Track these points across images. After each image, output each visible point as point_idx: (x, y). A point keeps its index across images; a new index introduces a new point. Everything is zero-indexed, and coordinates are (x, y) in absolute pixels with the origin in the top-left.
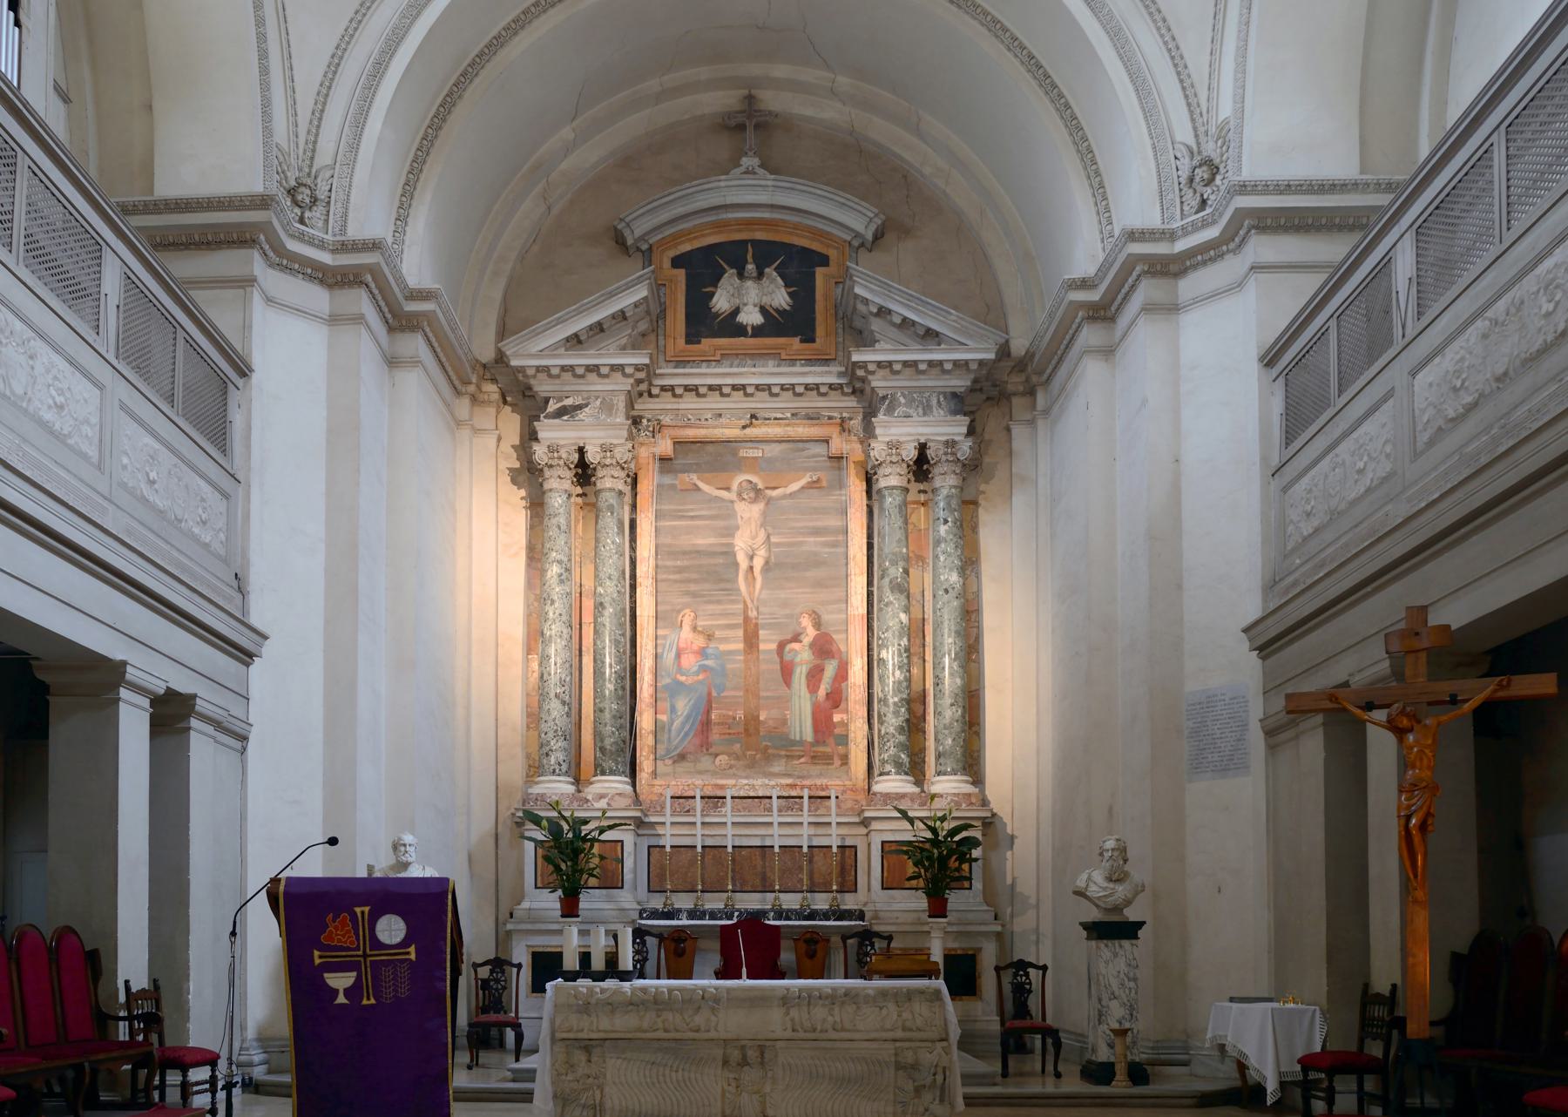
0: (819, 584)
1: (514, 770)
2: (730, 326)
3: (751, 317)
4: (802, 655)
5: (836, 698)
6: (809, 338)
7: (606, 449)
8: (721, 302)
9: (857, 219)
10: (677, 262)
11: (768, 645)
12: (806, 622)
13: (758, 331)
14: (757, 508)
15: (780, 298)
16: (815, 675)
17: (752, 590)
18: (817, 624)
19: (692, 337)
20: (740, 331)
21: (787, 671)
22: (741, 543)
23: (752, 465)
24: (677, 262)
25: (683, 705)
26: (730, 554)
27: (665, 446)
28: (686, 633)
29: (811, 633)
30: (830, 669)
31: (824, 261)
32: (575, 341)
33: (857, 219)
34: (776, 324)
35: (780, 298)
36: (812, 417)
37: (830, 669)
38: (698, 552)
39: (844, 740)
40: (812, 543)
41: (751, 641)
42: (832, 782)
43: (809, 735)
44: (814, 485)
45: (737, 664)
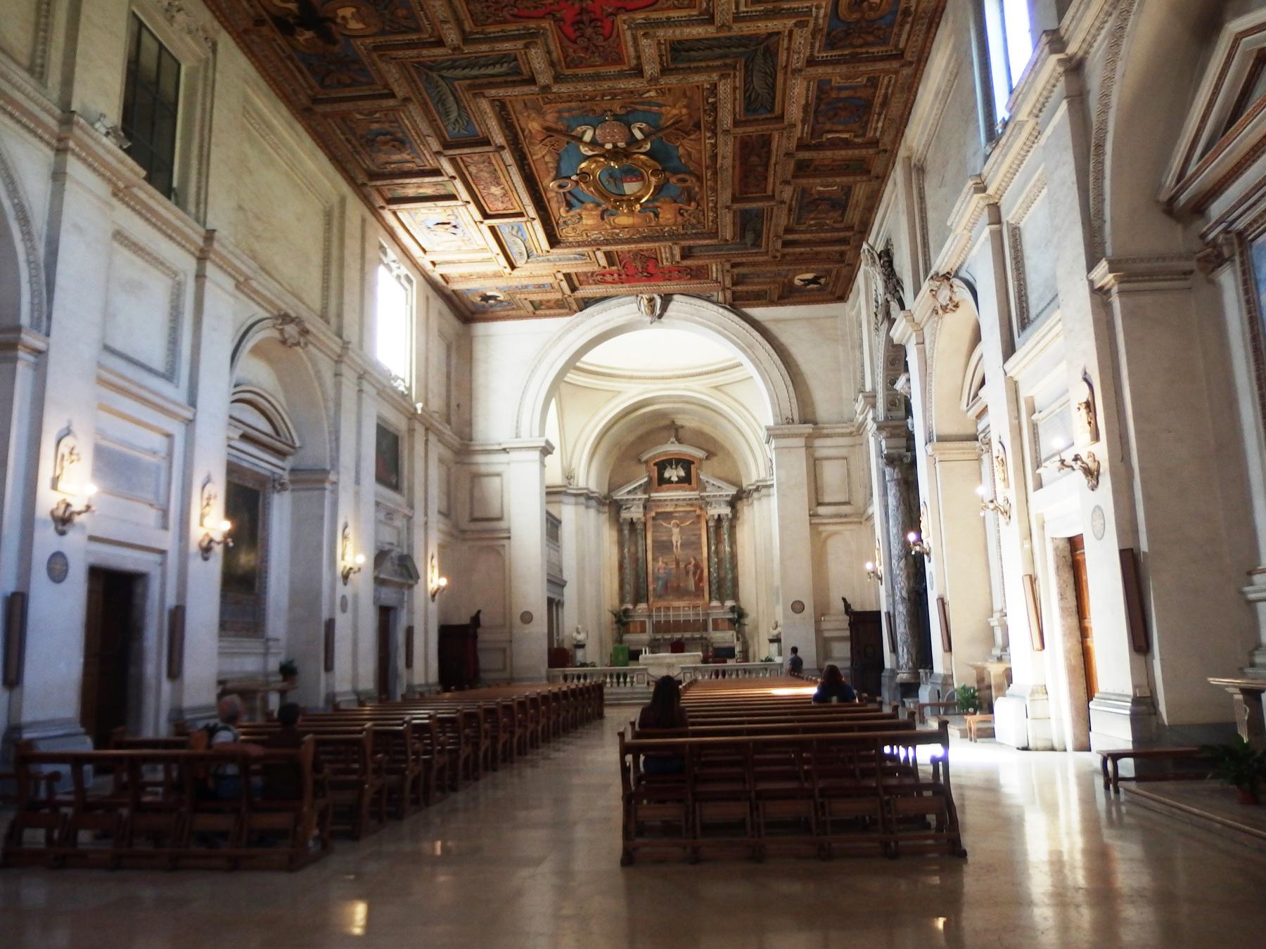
0: (696, 549)
1: (616, 602)
2: (669, 481)
3: (675, 479)
4: (691, 567)
5: (701, 579)
6: (690, 483)
7: (639, 519)
8: (667, 475)
9: (700, 454)
10: (655, 464)
11: (682, 565)
12: (692, 560)
13: (677, 482)
14: (678, 530)
15: (682, 473)
16: (695, 573)
17: (677, 551)
18: (695, 559)
19: (660, 484)
20: (672, 482)
21: (687, 573)
22: (674, 539)
23: (676, 518)
24: (655, 464)
25: (660, 583)
26: (671, 542)
27: (653, 514)
28: (660, 563)
29: (693, 562)
30: (699, 572)
31: (693, 463)
32: (629, 492)
33: (700, 454)
34: (681, 480)
35: (682, 473)
36: (692, 505)
37: (699, 572)
38: (663, 542)
39: (703, 590)
40: (693, 538)
41: (678, 564)
42: (700, 602)
43: (693, 589)
44: (692, 523)
45: (674, 571)
